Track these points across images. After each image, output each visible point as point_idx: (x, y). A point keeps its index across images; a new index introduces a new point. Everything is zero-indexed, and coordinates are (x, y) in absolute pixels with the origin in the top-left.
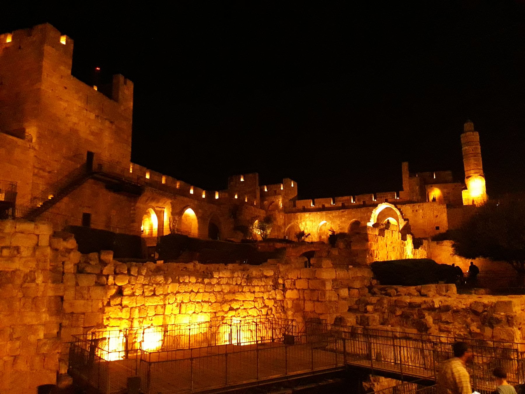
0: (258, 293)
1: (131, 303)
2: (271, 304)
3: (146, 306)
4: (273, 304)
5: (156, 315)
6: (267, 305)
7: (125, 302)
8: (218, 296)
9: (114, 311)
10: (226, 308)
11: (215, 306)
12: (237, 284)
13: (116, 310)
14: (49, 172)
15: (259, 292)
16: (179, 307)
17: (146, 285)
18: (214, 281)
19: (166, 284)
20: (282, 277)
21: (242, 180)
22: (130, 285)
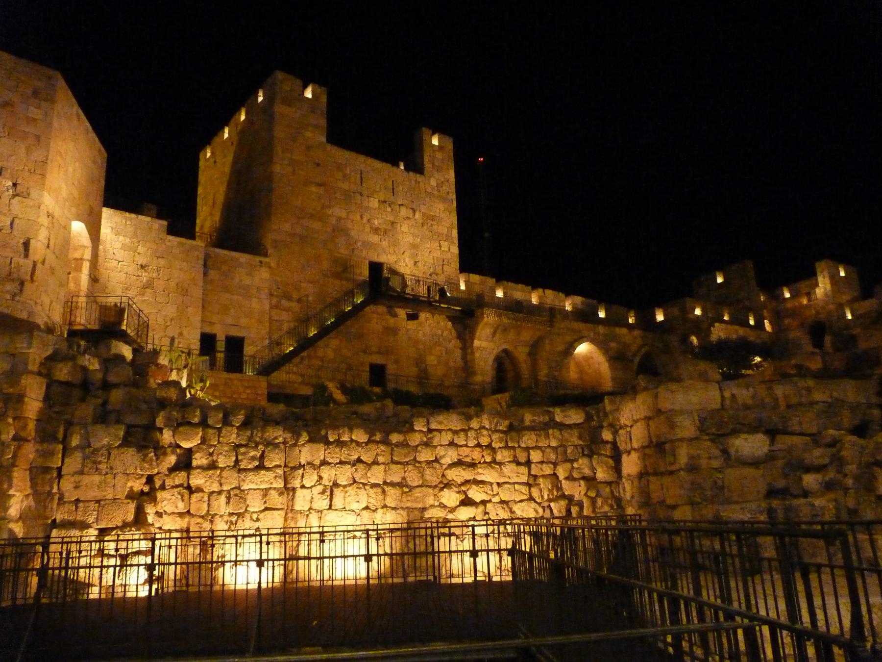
0: (539, 466)
1: (208, 484)
2: (577, 490)
3: (243, 491)
4: (583, 493)
5: (266, 509)
7: (197, 480)
8: (428, 472)
9: (171, 499)
10: (451, 498)
12: (479, 445)
14: (299, 301)
15: (542, 462)
16: (328, 493)
17: (241, 446)
18: (415, 439)
19: (295, 445)
21: (720, 280)
22: (205, 447)
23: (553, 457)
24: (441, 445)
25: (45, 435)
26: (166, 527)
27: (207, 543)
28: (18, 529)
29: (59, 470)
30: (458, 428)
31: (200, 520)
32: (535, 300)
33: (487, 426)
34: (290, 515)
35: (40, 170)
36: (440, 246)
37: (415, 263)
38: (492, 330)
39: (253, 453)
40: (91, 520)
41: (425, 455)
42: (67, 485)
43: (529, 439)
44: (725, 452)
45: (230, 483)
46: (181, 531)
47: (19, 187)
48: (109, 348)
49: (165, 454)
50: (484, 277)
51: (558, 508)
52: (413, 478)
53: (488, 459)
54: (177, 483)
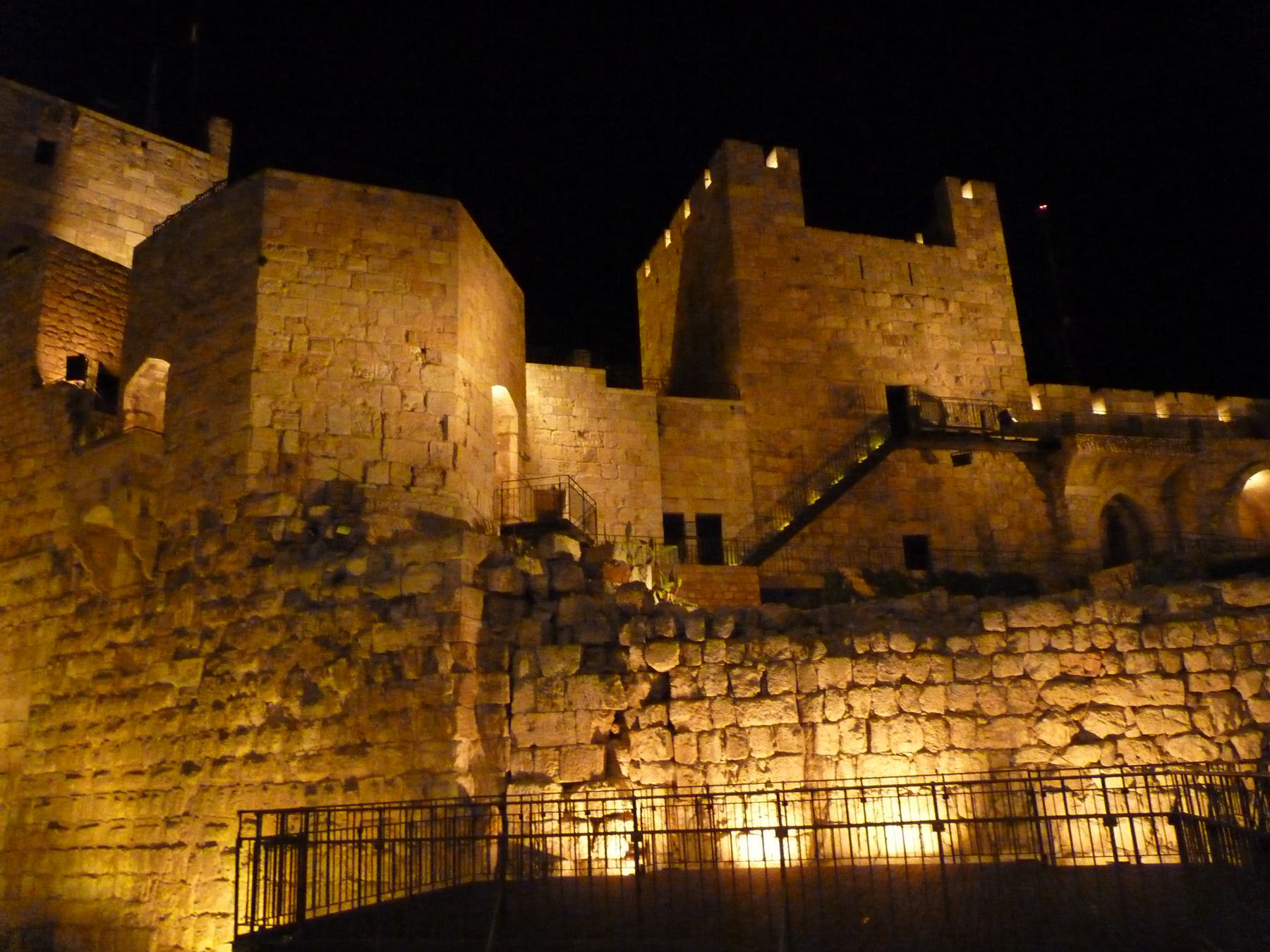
0: (1203, 677)
1: (695, 720)
3: (743, 729)
5: (777, 754)
6: (1259, 720)
7: (680, 716)
9: (647, 743)
10: (1055, 732)
11: (1003, 729)
13: (651, 741)
14: (790, 456)
15: (1207, 672)
16: (864, 730)
17: (733, 666)
18: (989, 644)
19: (809, 661)
23: (1226, 662)
24: (1031, 652)
25: (489, 665)
26: (646, 782)
27: (704, 802)
28: (468, 785)
29: (509, 707)
30: (1056, 624)
31: (689, 771)
32: (1161, 412)
33: (1105, 619)
34: (811, 762)
35: (450, 328)
36: (993, 349)
37: (957, 379)
38: (1093, 467)
40: (552, 772)
41: (1006, 669)
42: (519, 726)
43: (1180, 635)
45: (724, 719)
46: (665, 786)
48: (551, 543)
49: (635, 682)
50: (1069, 388)
52: (991, 704)
53: (1113, 670)
54: (654, 721)
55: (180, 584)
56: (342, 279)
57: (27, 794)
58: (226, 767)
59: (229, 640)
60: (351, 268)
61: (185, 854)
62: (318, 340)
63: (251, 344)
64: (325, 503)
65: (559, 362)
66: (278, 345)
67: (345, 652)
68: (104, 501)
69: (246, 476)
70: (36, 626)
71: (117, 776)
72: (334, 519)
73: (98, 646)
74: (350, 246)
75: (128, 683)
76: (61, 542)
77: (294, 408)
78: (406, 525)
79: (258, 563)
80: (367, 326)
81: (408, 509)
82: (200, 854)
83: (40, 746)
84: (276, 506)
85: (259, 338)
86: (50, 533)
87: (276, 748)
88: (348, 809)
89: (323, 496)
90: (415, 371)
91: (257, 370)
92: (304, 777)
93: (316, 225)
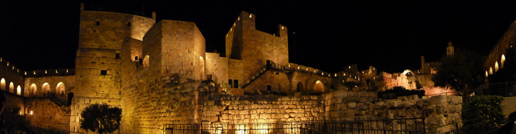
5: (245, 119)
7: (230, 112)
8: (281, 110)
10: (287, 116)
16: (259, 115)
17: (239, 105)
18: (278, 103)
19: (251, 104)
20: (324, 100)
25: (200, 103)
26: (224, 122)
27: (233, 126)
28: (196, 122)
31: (231, 121)
34: (250, 120)
35: (193, 46)
39: (242, 106)
41: (281, 107)
42: (204, 113)
43: (305, 103)
44: (347, 106)
46: (227, 123)
47: (189, 51)
48: (210, 84)
49: (223, 107)
51: (311, 118)
52: (278, 112)
55: (153, 91)
56: (175, 39)
57: (135, 120)
58: (161, 118)
59: (160, 99)
60: (176, 36)
61: (156, 129)
62: (171, 50)
63: (161, 51)
64: (173, 77)
65: (212, 52)
66: (165, 51)
67: (177, 101)
68: (142, 78)
69: (161, 73)
70: (134, 97)
71: (146, 118)
72: (175, 80)
73: (143, 100)
74: (176, 33)
75: (147, 105)
76: (137, 85)
77: (168, 62)
78: (186, 81)
79: (164, 87)
80: (179, 47)
81: (187, 78)
82: (158, 129)
83: (136, 114)
84: (166, 78)
85: (162, 50)
86: (135, 84)
87: (168, 115)
88: (179, 124)
89: (173, 76)
90: (187, 54)
91: (162, 56)
92: (172, 119)
93: (170, 29)
